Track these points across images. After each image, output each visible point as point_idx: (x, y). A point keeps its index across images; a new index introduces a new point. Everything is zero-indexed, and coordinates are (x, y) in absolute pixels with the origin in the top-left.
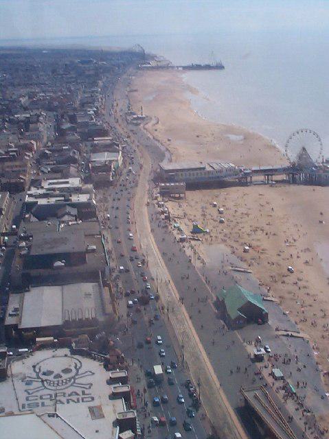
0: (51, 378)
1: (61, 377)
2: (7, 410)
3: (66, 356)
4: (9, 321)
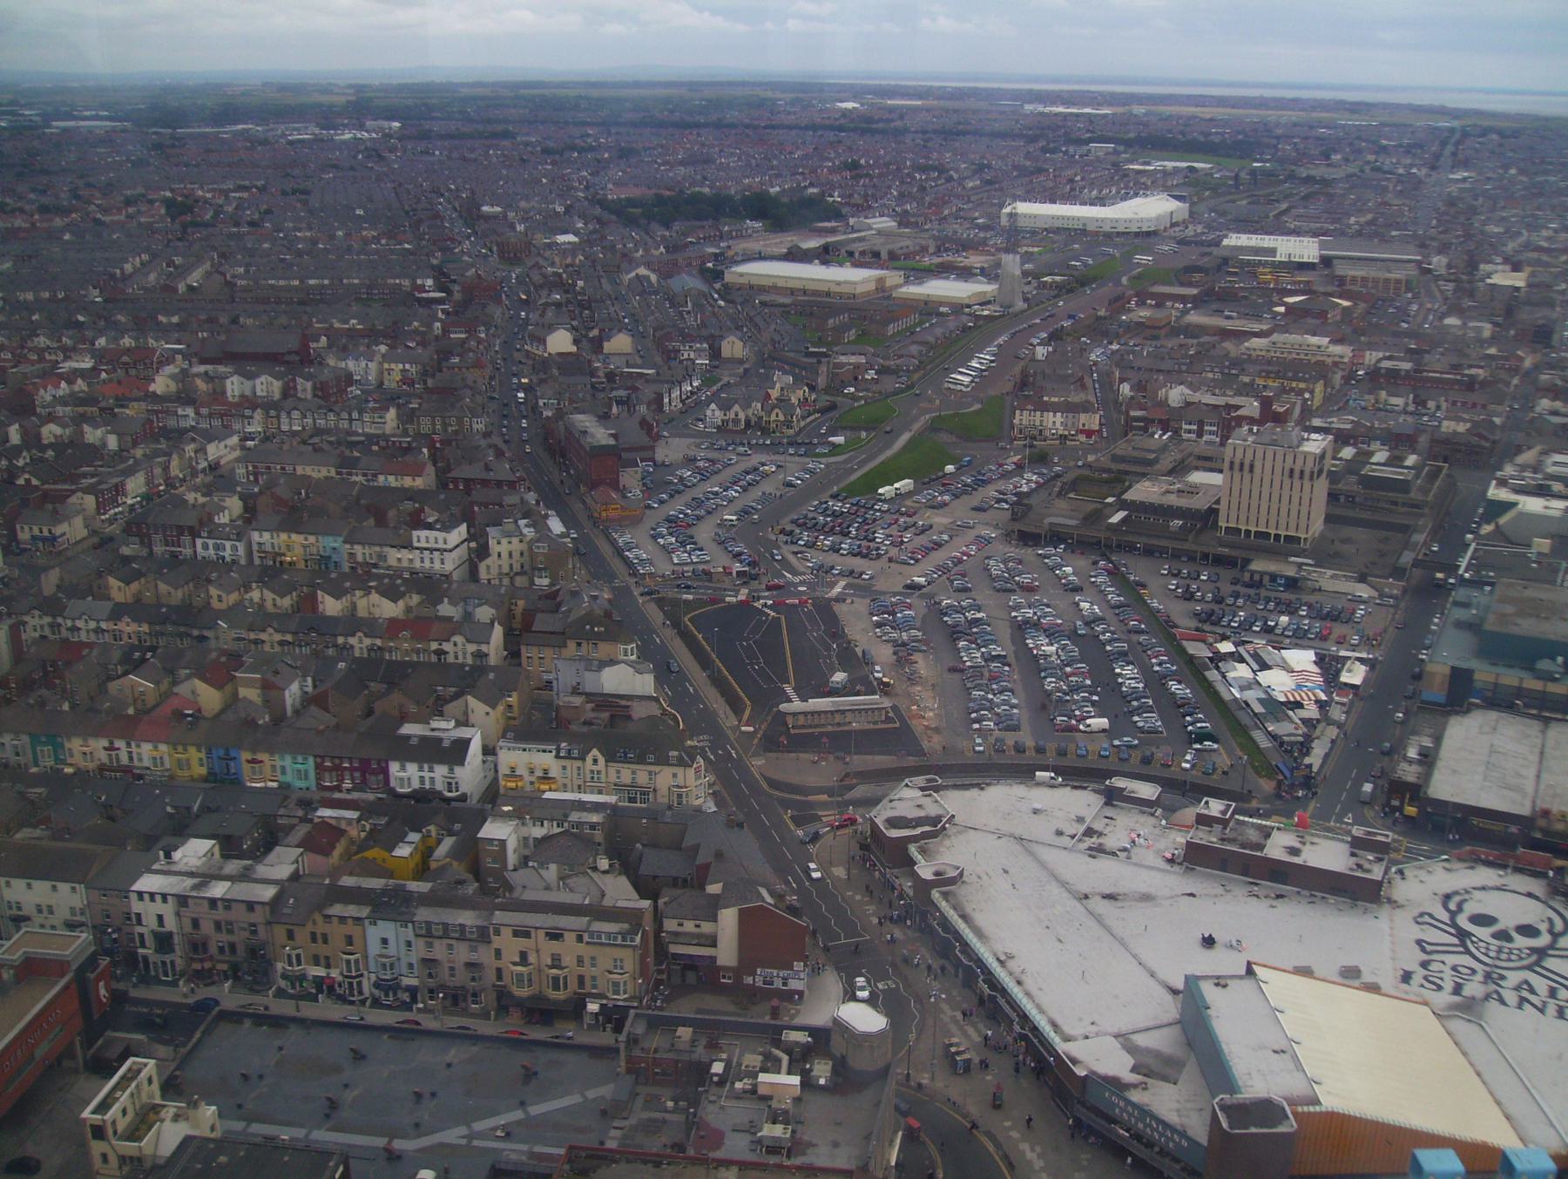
0: (1483, 933)
1: (1509, 939)
2: (1367, 977)
3: (1530, 895)
4: (1408, 773)
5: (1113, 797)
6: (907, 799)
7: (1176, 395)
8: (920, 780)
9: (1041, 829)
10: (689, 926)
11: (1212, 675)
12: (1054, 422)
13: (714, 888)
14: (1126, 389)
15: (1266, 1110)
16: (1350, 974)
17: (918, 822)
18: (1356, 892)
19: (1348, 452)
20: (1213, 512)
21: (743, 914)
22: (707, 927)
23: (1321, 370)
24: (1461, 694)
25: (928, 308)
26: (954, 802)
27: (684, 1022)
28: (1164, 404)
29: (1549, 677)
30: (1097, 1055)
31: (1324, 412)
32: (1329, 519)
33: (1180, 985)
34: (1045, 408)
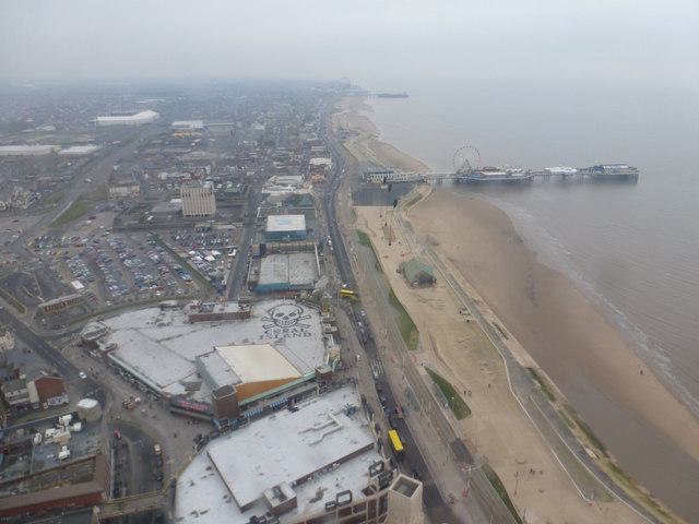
0: (281, 318)
4: (251, 278)
5: (163, 307)
6: (92, 326)
7: (163, 176)
8: (96, 318)
9: (141, 324)
10: (16, 393)
11: (189, 262)
12: (124, 191)
13: (22, 377)
14: (147, 176)
15: (228, 389)
16: (246, 341)
17: (98, 332)
18: (244, 316)
19: (220, 186)
20: (181, 211)
21: (36, 382)
22: (23, 391)
23: (208, 162)
24: (263, 252)
25: (73, 158)
26: (109, 323)
27: (19, 428)
28: (160, 179)
29: (285, 242)
30: (176, 390)
31: (210, 175)
32: (217, 207)
33: (194, 359)
34: (119, 186)
